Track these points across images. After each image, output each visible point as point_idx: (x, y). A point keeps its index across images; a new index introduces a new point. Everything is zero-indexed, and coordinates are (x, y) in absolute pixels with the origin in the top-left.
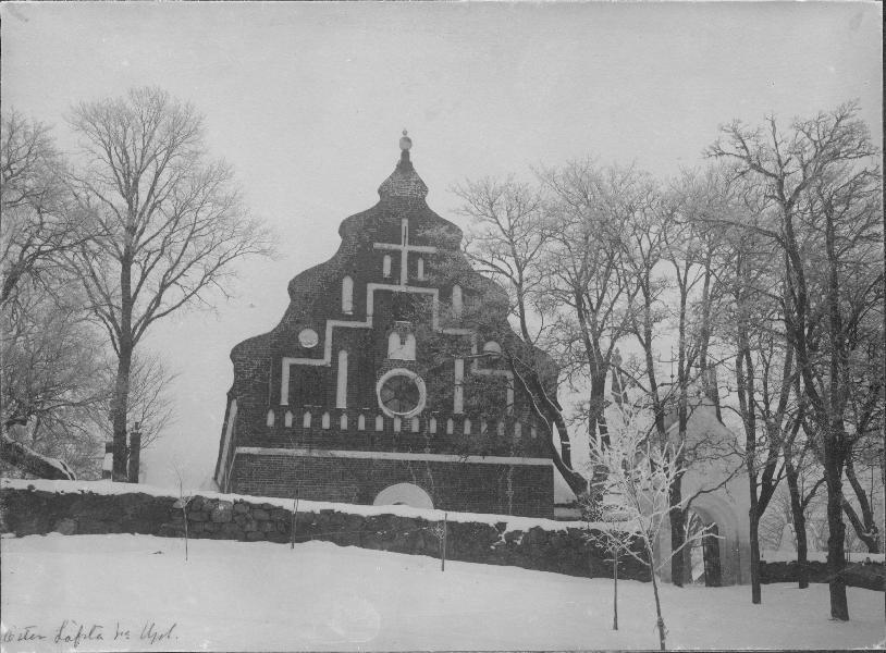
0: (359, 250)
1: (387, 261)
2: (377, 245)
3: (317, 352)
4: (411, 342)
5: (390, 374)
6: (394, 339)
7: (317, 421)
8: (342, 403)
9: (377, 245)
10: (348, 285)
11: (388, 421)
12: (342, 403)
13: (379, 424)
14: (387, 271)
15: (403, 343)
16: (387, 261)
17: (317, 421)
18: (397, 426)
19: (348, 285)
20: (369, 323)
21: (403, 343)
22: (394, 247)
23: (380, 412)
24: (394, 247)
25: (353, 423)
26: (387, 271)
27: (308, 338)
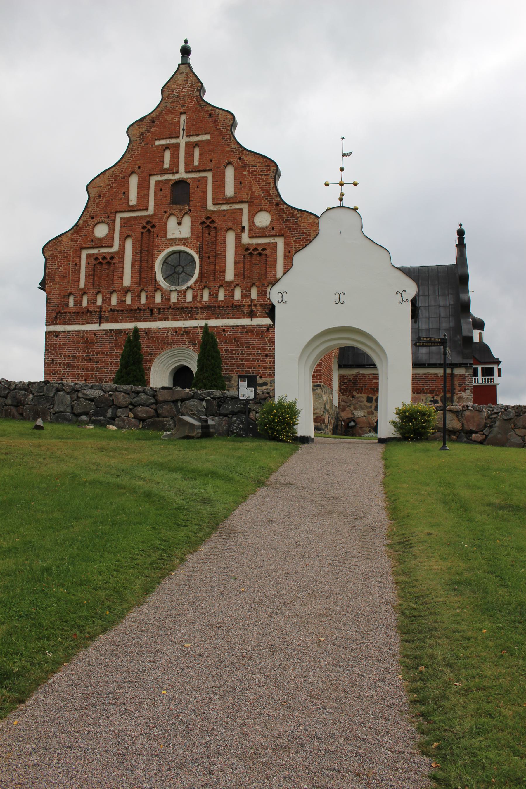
0: (142, 148)
1: (167, 155)
2: (157, 143)
3: (107, 242)
4: (187, 221)
5: (167, 251)
6: (172, 222)
7: (107, 300)
8: (127, 282)
9: (157, 143)
10: (134, 181)
11: (166, 296)
12: (127, 282)
13: (158, 299)
14: (167, 164)
15: (180, 224)
16: (167, 155)
17: (107, 300)
18: (173, 298)
19: (134, 181)
20: (151, 210)
21: (180, 224)
22: (173, 141)
23: (157, 288)
24: (173, 141)
25: (136, 298)
26: (167, 164)
27: (101, 231)
